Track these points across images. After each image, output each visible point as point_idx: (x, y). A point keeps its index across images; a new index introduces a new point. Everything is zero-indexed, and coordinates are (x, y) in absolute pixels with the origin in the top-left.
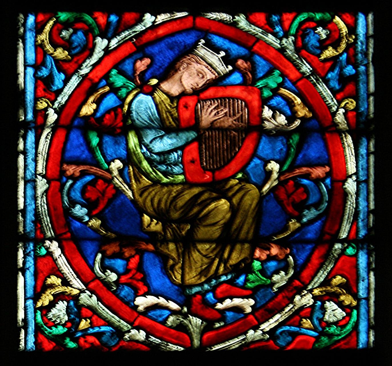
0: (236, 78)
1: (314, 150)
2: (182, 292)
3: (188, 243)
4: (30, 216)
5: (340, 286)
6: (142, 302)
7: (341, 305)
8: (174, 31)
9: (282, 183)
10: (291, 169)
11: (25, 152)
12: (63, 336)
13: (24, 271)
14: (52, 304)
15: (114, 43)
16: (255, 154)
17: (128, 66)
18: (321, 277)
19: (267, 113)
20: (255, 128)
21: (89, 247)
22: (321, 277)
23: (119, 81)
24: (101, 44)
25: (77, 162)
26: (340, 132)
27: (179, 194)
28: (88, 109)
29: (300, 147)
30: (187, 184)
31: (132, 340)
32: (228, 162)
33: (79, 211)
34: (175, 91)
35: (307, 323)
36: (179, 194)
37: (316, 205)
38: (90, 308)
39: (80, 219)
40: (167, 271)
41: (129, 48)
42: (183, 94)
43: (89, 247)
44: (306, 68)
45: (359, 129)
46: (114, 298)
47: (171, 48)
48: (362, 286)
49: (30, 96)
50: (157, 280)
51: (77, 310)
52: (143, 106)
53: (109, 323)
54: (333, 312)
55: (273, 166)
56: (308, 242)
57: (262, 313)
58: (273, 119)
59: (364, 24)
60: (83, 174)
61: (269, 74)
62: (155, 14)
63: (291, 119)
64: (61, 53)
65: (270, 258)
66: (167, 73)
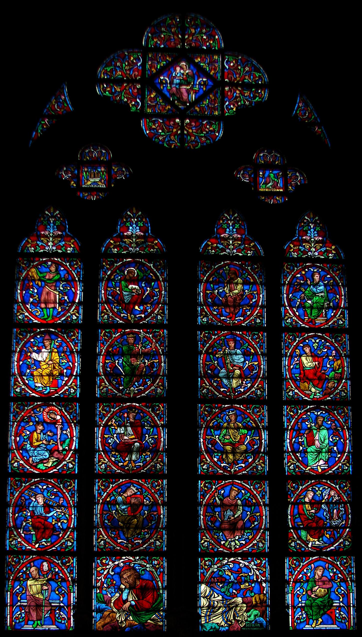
0: (139, 493)
1: (154, 509)
2: (127, 539)
3: (128, 529)
4: (96, 522)
5: (159, 538)
6: (119, 541)
7: (159, 542)
8: (126, 483)
9: (148, 515)
10: (150, 512)
11: (95, 509)
12: (103, 548)
13: (95, 534)
14: (101, 541)
15: (114, 485)
16: (142, 509)
17: (117, 490)
18: (155, 536)
19: (145, 501)
20: (142, 504)
21: (108, 529)
22: (155, 536)
23: (115, 493)
24: (111, 485)
25: (106, 511)
26: (160, 505)
27: (127, 518)
28: (108, 500)
29: (151, 508)
30: (128, 516)
31: (117, 549)
32: (136, 511)
33: (106, 521)
34: (126, 495)
35: (153, 546)
36: (127, 518)
37: (155, 521)
38: (108, 542)
39: (106, 523)
40: (124, 534)
41: (117, 487)
42: (128, 496)
43: (108, 529)
44: (153, 491)
45: (164, 504)
46: (113, 540)
47: (125, 486)
48: (164, 538)
49: (96, 497)
50: (122, 536)
51: (106, 543)
52: (120, 499)
53: (112, 545)
54: (158, 543)
55: (146, 512)
56: (153, 528)
57: (144, 543)
58: (146, 502)
59: (165, 482)
60: (107, 513)
61: (145, 492)
62: (122, 479)
63: (150, 502)
64: (103, 487)
65: (145, 532)
66: (125, 492)
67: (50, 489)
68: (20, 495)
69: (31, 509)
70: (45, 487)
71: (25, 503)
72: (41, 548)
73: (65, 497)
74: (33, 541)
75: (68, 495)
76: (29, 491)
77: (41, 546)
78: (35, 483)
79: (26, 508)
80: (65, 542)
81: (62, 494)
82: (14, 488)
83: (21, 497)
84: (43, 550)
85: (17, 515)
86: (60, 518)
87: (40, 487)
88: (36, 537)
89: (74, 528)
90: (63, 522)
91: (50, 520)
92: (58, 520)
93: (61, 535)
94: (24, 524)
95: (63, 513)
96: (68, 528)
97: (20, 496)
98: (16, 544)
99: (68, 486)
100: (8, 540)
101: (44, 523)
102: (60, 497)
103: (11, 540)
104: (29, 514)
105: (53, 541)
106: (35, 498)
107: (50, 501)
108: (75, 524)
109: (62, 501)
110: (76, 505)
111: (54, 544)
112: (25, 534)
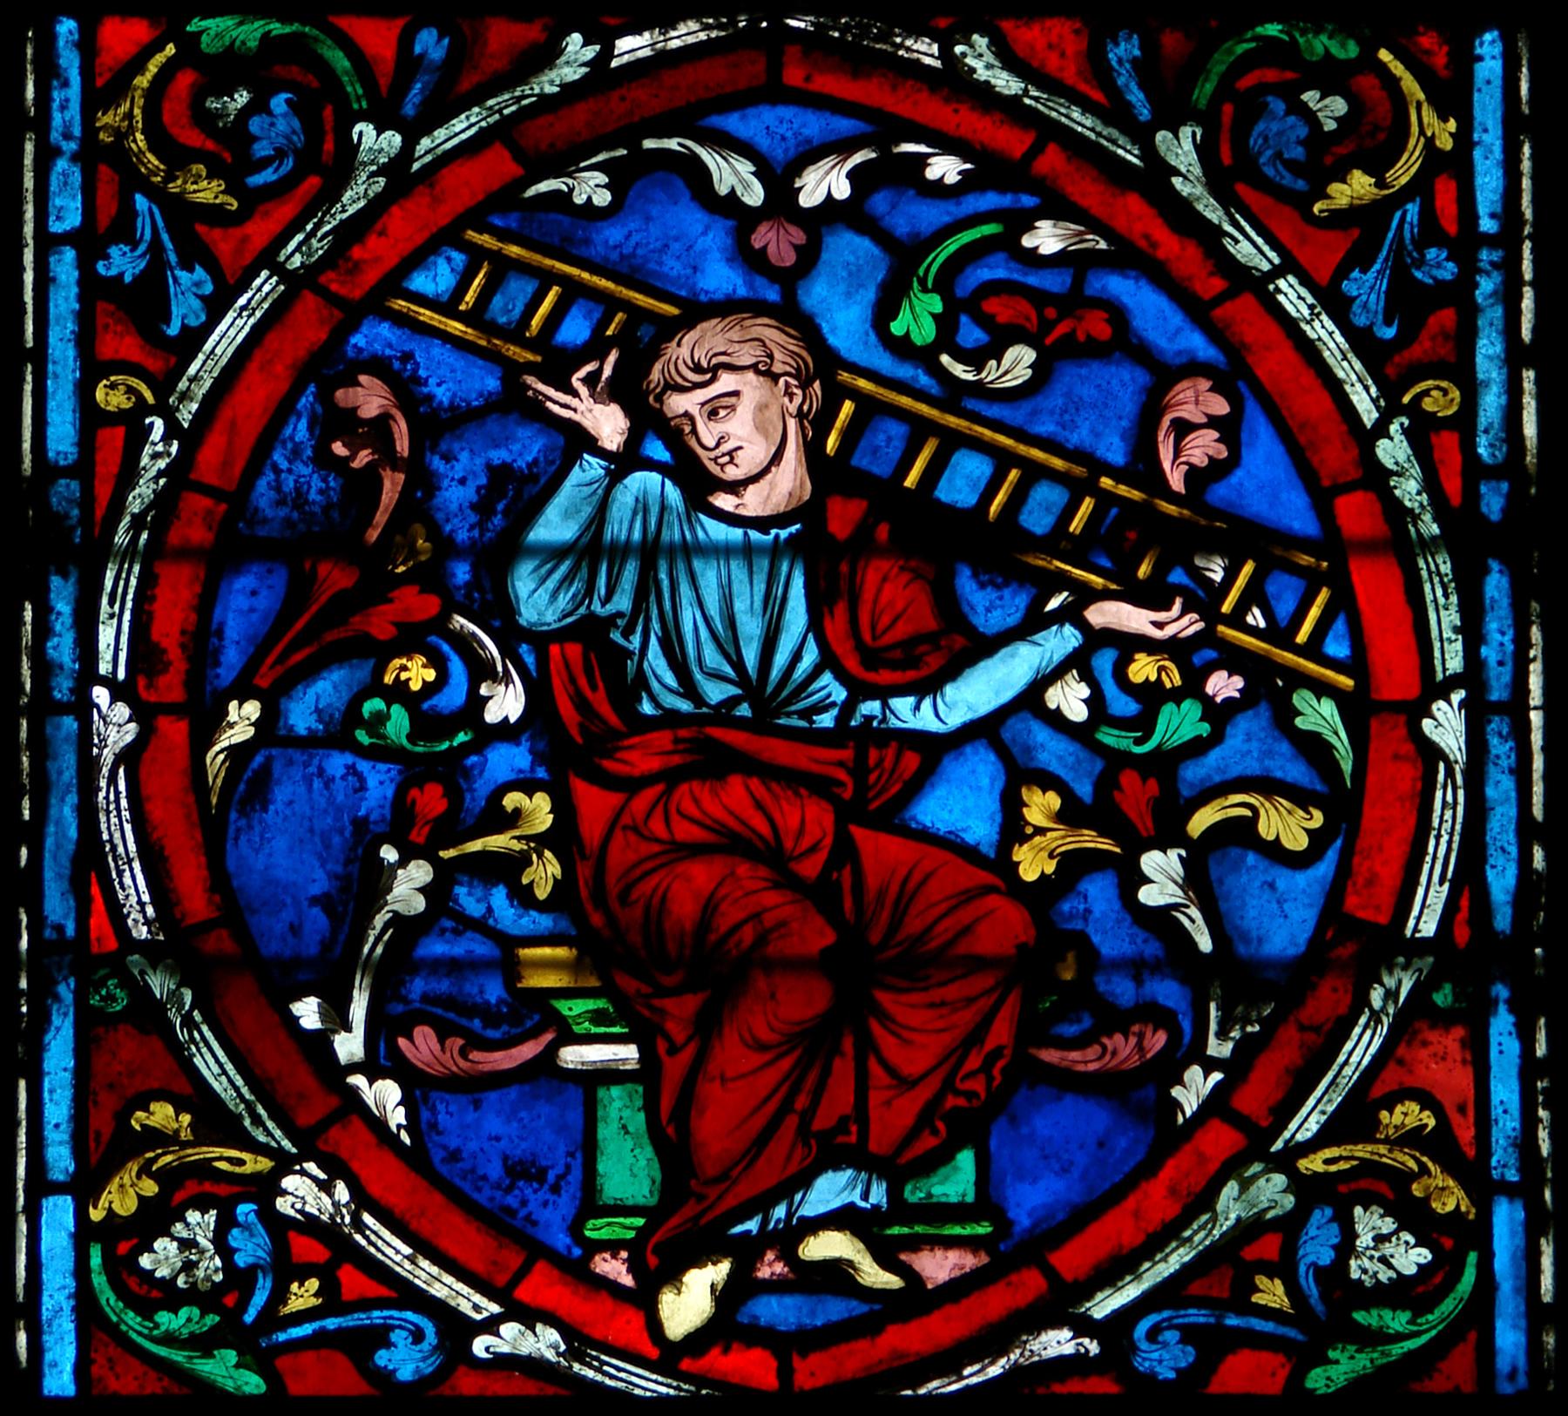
67: (931, 215)
68: (310, 326)
69: (538, 599)
70: (825, 183)
71: (421, 482)
72: (787, 1345)
73: (1274, 364)
74: (591, 1205)
75: (1324, 332)
76: (502, 268)
77: (774, 1311)
78: (611, 113)
79: (431, 577)
80: (1292, 1225)
81: (1197, 311)
82: (180, 212)
83: (332, 366)
84: (813, 1372)
85: (243, 718)
86: (1168, 761)
87: (733, 175)
88: (670, 1141)
89: (1469, 955)
90: (1240, 832)
91: (959, 806)
92: (1133, 797)
93: (1194, 1090)
94: (409, 887)
95: (1234, 660)
96: (1355, 940)
97: (312, 353)
98: (239, 1279)
99: (1326, 158)
100: (59, 1214)
101: (844, 851)
102: (1165, 374)
103: (122, 1196)
104: (506, 703)
105: (1028, 1201)
106: (628, 391)
107: (952, 442)
108: (1501, 880)
109: (1203, 447)
110: (1493, 501)
111: (1071, 1260)
112: (416, 1086)
